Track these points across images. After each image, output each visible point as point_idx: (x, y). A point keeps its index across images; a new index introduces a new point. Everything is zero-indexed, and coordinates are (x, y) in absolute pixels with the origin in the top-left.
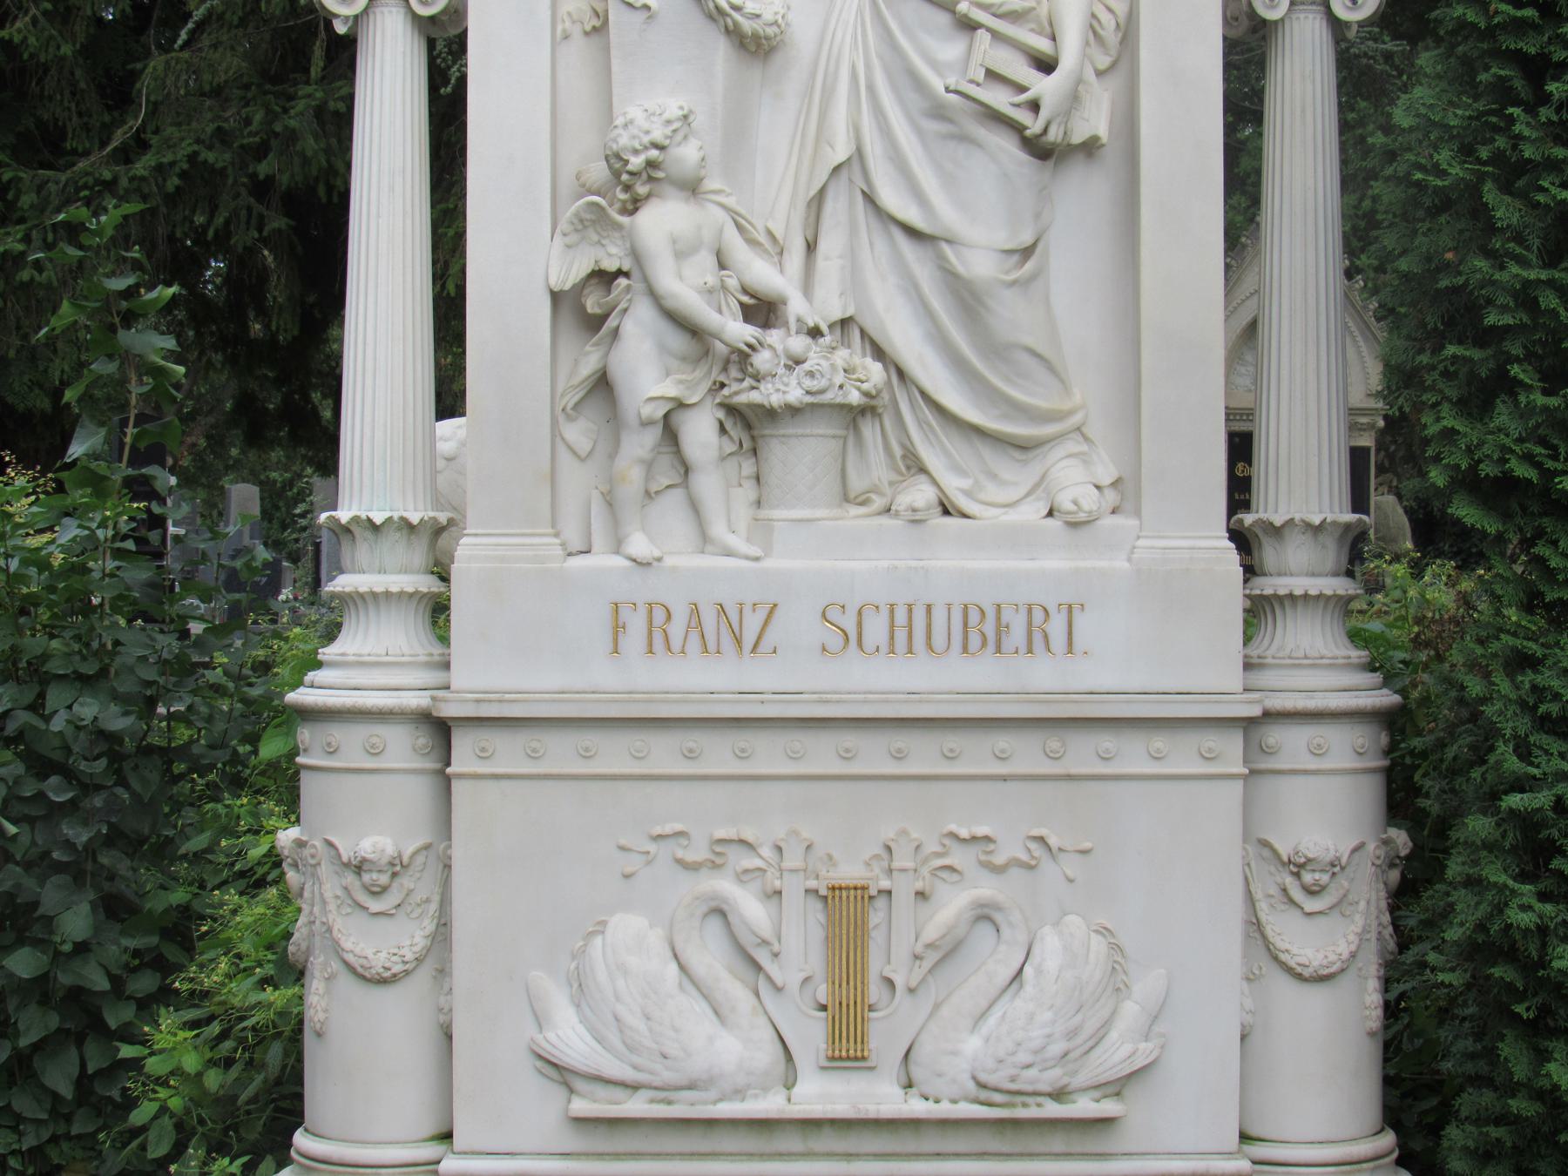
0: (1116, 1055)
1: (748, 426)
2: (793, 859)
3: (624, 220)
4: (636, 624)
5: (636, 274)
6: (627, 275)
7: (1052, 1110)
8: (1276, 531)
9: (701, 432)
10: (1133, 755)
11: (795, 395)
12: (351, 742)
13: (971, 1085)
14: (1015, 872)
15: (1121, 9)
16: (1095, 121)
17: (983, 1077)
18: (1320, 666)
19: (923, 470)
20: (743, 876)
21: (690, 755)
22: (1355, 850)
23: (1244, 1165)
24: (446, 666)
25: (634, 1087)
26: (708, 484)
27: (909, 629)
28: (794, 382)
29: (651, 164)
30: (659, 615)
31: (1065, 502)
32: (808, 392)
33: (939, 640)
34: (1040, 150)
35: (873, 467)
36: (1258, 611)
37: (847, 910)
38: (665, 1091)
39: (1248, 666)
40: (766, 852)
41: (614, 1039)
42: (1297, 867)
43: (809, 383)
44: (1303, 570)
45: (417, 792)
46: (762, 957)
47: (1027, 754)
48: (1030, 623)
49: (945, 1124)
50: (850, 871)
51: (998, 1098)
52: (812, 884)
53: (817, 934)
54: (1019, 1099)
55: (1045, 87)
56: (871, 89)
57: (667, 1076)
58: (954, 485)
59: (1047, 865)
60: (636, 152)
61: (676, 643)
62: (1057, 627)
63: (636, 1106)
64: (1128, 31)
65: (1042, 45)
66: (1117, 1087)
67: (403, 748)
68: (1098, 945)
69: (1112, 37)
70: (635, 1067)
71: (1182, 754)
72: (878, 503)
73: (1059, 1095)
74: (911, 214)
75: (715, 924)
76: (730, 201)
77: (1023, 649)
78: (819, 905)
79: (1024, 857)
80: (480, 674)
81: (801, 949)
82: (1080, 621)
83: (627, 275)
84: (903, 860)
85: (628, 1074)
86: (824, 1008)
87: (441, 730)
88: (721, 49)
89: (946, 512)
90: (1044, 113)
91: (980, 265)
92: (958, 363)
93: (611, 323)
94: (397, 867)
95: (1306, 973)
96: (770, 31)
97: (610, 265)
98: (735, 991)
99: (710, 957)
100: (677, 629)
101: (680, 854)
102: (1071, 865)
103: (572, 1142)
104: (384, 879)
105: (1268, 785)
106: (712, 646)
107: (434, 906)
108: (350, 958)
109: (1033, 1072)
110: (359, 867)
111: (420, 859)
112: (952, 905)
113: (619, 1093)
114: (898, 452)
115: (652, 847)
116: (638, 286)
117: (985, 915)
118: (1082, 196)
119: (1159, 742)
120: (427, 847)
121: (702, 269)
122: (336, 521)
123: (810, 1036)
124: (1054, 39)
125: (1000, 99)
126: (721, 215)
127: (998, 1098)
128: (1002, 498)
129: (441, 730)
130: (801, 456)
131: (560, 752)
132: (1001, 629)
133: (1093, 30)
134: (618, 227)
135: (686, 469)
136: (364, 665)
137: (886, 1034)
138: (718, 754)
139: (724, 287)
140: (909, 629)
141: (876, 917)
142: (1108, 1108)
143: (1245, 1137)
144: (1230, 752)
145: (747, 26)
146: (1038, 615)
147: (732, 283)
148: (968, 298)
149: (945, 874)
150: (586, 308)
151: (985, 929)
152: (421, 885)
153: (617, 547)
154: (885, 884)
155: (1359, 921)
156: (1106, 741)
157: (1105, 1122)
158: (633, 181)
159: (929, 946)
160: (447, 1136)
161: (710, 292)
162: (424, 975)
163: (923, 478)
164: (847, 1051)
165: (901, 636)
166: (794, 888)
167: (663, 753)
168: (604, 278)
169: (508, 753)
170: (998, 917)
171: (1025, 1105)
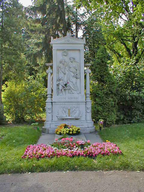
8: (87, 94)
9: (63, 90)
10: (81, 103)
16: (79, 77)
18: (89, 99)
26: (63, 92)
27: (71, 98)
34: (77, 78)
37: (69, 110)
38: (62, 117)
44: (88, 95)
45: (51, 105)
47: (76, 103)
50: (69, 108)
55: (77, 76)
66: (81, 117)
67: (50, 103)
74: (71, 81)
87: (52, 103)
88: (63, 74)
91: (74, 83)
92: (73, 87)
110: (49, 109)
112: (73, 110)
117: (75, 110)
118: (78, 80)
121: (63, 84)
123: (68, 115)
125: (75, 76)
130: (67, 91)
133: (79, 73)
135: (62, 92)
137: (71, 115)
138: (64, 103)
140: (71, 98)
143: (86, 119)
144: (85, 103)
148: (74, 84)
150: (58, 85)
152: (51, 109)
158: (59, 80)
168: (59, 84)
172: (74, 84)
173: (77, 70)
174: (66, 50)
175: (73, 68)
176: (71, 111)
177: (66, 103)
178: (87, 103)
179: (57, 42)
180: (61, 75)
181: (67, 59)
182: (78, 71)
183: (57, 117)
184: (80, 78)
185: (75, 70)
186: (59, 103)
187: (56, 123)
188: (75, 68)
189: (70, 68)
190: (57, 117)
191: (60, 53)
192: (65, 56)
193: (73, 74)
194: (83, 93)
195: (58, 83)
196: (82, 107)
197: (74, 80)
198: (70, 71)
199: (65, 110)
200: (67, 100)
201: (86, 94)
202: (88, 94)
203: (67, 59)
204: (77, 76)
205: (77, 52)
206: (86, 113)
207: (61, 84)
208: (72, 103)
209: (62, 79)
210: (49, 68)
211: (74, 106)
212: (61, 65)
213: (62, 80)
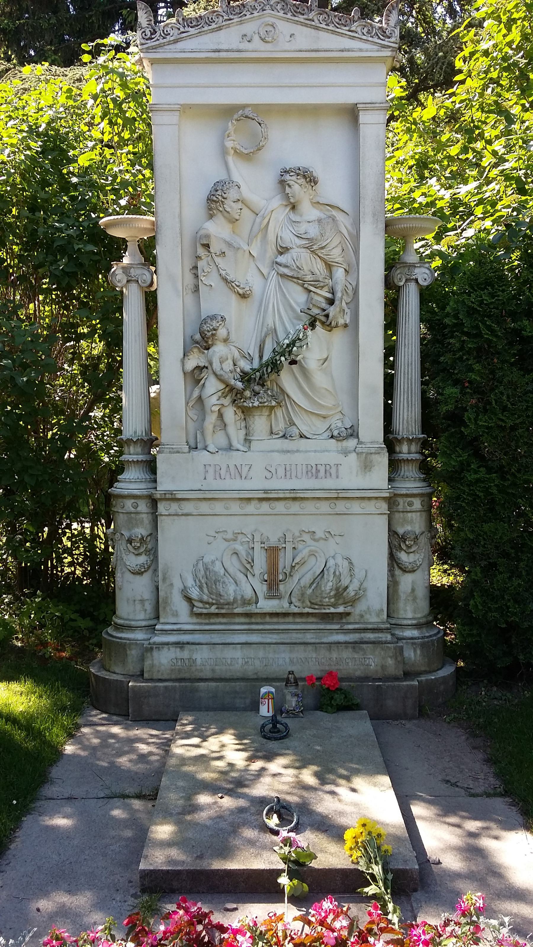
1: (243, 412)
2: (257, 538)
3: (206, 351)
4: (211, 470)
5: (209, 367)
6: (207, 368)
7: (332, 610)
10: (356, 507)
11: (256, 404)
12: (129, 504)
13: (309, 604)
14: (322, 542)
15: (354, 284)
17: (313, 601)
19: (294, 424)
20: (242, 543)
21: (227, 508)
22: (423, 533)
23: (389, 626)
24: (155, 481)
25: (213, 604)
28: (256, 399)
29: (213, 335)
30: (218, 468)
31: (335, 433)
32: (261, 403)
33: (299, 475)
36: (394, 465)
37: (273, 552)
38: (220, 606)
39: (390, 480)
40: (250, 536)
41: (205, 590)
42: (403, 538)
43: (260, 400)
45: (146, 518)
46: (248, 566)
47: (324, 507)
48: (326, 470)
49: (301, 615)
50: (273, 541)
51: (316, 607)
52: (263, 545)
53: (264, 559)
54: (323, 607)
56: (278, 310)
57: (222, 601)
58: (304, 429)
59: (331, 539)
60: (208, 331)
61: (223, 477)
62: (333, 471)
63: (213, 609)
64: (356, 291)
65: (329, 296)
67: (143, 507)
68: (346, 563)
69: (350, 292)
70: (213, 599)
71: (371, 507)
72: (281, 434)
73: (334, 606)
75: (235, 557)
76: (237, 345)
77: (324, 477)
78: (265, 551)
79: (324, 537)
81: (260, 563)
82: (340, 468)
83: (207, 368)
84: (289, 538)
85: (211, 600)
86: (266, 581)
88: (234, 299)
89: (301, 437)
90: (330, 318)
93: (202, 382)
94: (142, 540)
95: (407, 570)
96: (248, 293)
97: (202, 364)
98: (241, 577)
99: (234, 566)
100: (223, 472)
101: (224, 537)
102: (337, 539)
103: (195, 620)
104: (138, 545)
105: (397, 515)
106: (233, 476)
107: (152, 552)
108: (129, 567)
109: (327, 600)
111: (149, 538)
113: (207, 606)
114: (287, 419)
115: (217, 535)
116: (210, 371)
117: (312, 554)
119: (365, 504)
120: (151, 535)
121: (228, 366)
122: (122, 439)
123: (262, 589)
124: (333, 294)
126: (233, 348)
127: (316, 607)
129: (154, 502)
131: (188, 507)
132: (318, 471)
134: (203, 353)
139: (235, 370)
141: (281, 554)
142: (349, 609)
143: (388, 616)
144: (384, 507)
145: (241, 292)
146: (328, 467)
147: (238, 370)
149: (301, 542)
151: (313, 559)
153: (205, 448)
154: (284, 545)
155: (423, 555)
156: (348, 504)
157: (348, 614)
159: (298, 563)
160: (158, 618)
161: (231, 372)
162: (150, 572)
163: (295, 427)
165: (288, 474)
166: (257, 546)
167: (218, 508)
168: (200, 369)
169: (174, 507)
170: (316, 554)
171: (324, 609)
173: (329, 266)
175: (305, 255)
176: (285, 561)
177: (251, 508)
178: (402, 503)
179: (180, 45)
182: (339, 273)
183: (189, 599)
184: (353, 327)
185: (319, 268)
186: (204, 508)
187: (180, 645)
189: (283, 250)
190: (189, 599)
194: (372, 429)
195: (191, 364)
198: (283, 276)
201: (391, 442)
202: (410, 441)
204: (332, 311)
206: (391, 571)
207: (216, 366)
208: (295, 507)
209: (222, 332)
211: (308, 524)
212: (217, 229)
213: (226, 340)
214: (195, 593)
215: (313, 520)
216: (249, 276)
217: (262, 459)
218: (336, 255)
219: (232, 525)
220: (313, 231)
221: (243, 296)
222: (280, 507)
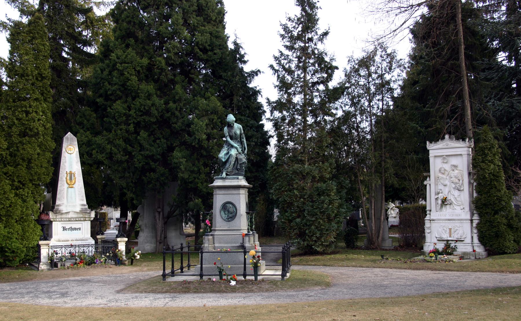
0: (464, 236)
10: (465, 221)
27: (453, 215)
35: (452, 206)
37: (450, 229)
47: (459, 221)
80: (432, 218)
81: (448, 231)
99: (444, 232)
118: (462, 193)
123: (448, 236)
128: (458, 208)
131: (436, 221)
136: (428, 217)
138: (444, 221)
148: (456, 198)
150: (437, 199)
158: (438, 193)
164: (450, 236)
167: (441, 221)
172: (456, 198)
174: (446, 156)
176: (452, 231)
177: (447, 221)
178: (474, 221)
180: (440, 187)
181: (447, 167)
182: (461, 181)
185: (457, 181)
186: (439, 221)
188: (456, 177)
191: (439, 161)
192: (446, 163)
193: (454, 186)
195: (436, 197)
196: (468, 225)
197: (456, 193)
199: (445, 229)
200: (448, 217)
203: (447, 167)
205: (459, 158)
208: (454, 221)
210: (428, 179)
212: (440, 175)
214: (437, 236)
215: (457, 224)
216: (447, 182)
217: (447, 212)
218: (460, 178)
219: (444, 224)
220: (455, 175)
221: (445, 186)
222: (451, 221)
